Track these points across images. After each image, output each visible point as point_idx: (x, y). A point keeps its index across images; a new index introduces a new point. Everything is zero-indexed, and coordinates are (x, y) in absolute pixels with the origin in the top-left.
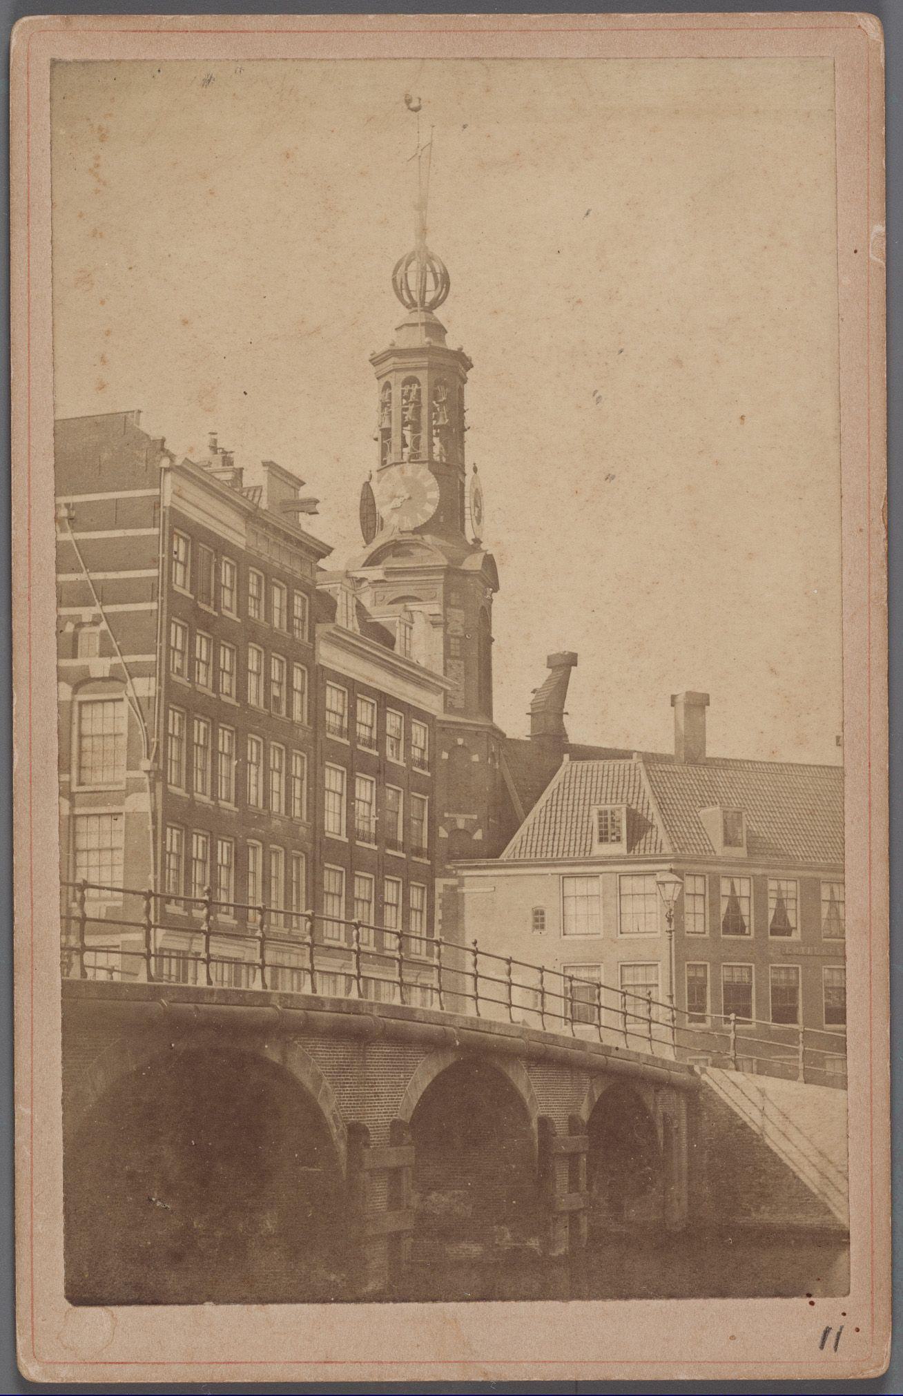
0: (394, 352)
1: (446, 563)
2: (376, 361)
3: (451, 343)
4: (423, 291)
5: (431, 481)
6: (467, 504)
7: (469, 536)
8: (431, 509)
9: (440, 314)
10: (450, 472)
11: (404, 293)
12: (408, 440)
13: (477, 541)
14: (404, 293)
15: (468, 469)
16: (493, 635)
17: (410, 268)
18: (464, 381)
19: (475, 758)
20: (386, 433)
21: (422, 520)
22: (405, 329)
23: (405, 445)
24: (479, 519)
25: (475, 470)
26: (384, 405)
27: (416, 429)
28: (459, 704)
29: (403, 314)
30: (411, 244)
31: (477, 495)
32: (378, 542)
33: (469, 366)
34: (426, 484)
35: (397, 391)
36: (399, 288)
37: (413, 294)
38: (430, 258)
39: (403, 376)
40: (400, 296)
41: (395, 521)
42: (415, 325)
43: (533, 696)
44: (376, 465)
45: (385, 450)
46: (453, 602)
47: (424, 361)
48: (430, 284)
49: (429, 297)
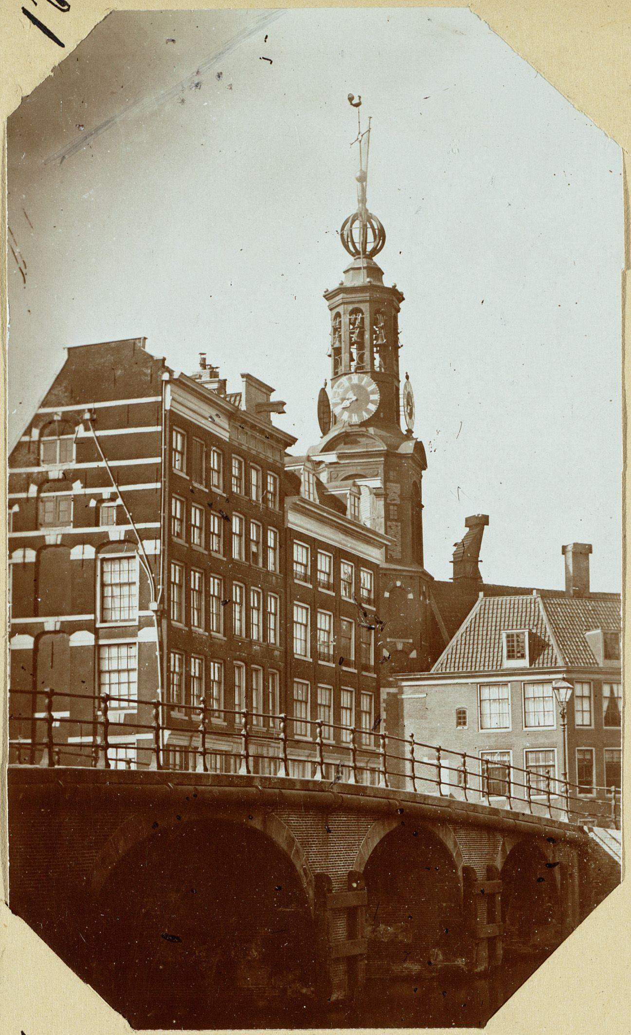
0: (342, 290)
1: (386, 448)
2: (328, 296)
3: (387, 282)
4: (365, 243)
5: (374, 386)
6: (402, 402)
7: (404, 428)
8: (373, 408)
9: (377, 259)
10: (388, 379)
11: (350, 244)
12: (355, 356)
13: (410, 431)
14: (350, 244)
15: (402, 377)
17: (354, 226)
18: (398, 310)
19: (411, 596)
20: (337, 351)
21: (366, 416)
22: (351, 272)
23: (352, 360)
24: (411, 415)
25: (407, 377)
26: (336, 330)
27: (361, 347)
28: (397, 555)
29: (349, 261)
30: (354, 208)
31: (409, 398)
32: (334, 432)
33: (400, 298)
34: (370, 389)
35: (345, 319)
36: (346, 241)
37: (357, 245)
39: (350, 307)
40: (347, 247)
41: (346, 418)
42: (359, 268)
43: (455, 548)
44: (330, 375)
45: (337, 364)
46: (392, 478)
47: (366, 296)
49: (369, 247)
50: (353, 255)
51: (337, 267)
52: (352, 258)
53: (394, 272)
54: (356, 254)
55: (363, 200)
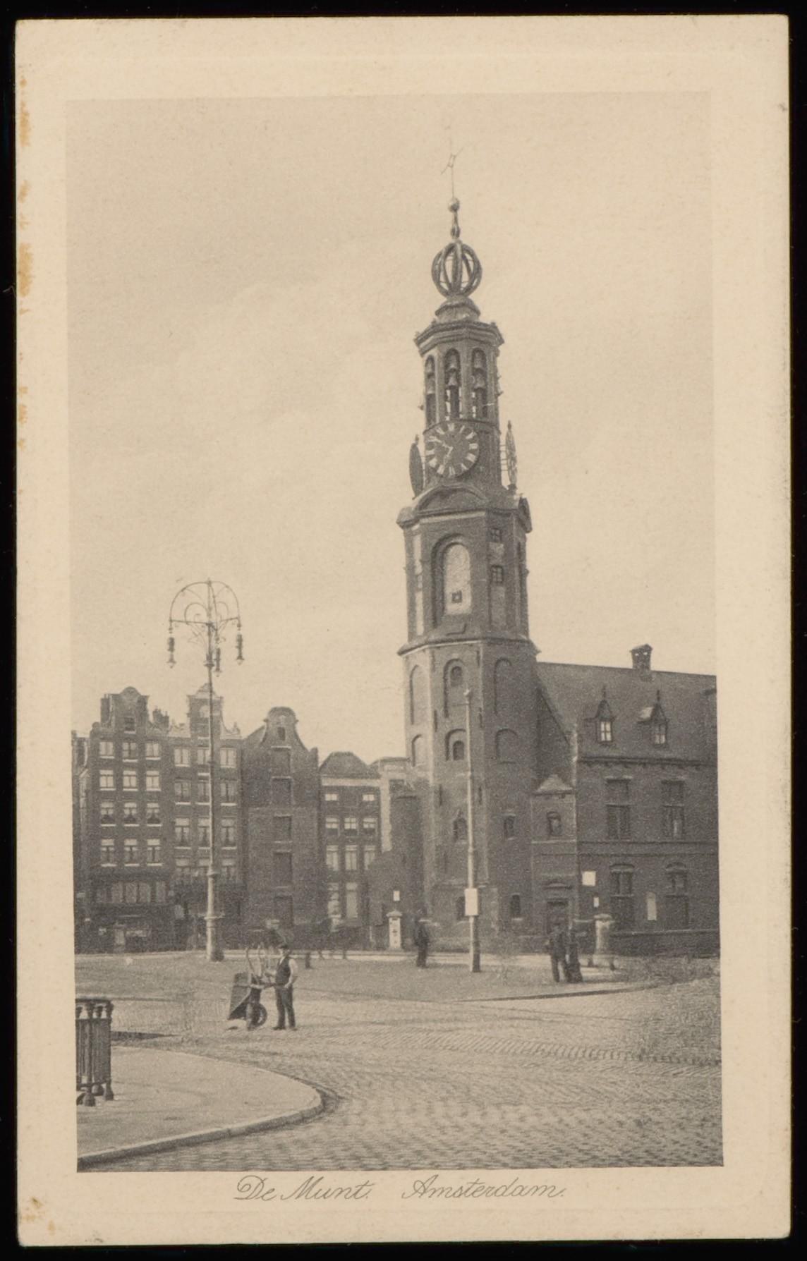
0: (434, 329)
7: (506, 482)
13: (513, 487)
15: (503, 427)
18: (497, 354)
20: (430, 398)
24: (513, 472)
25: (509, 426)
29: (442, 300)
31: (511, 448)
38: (466, 249)
40: (438, 282)
48: (465, 277)
55: (456, 233)
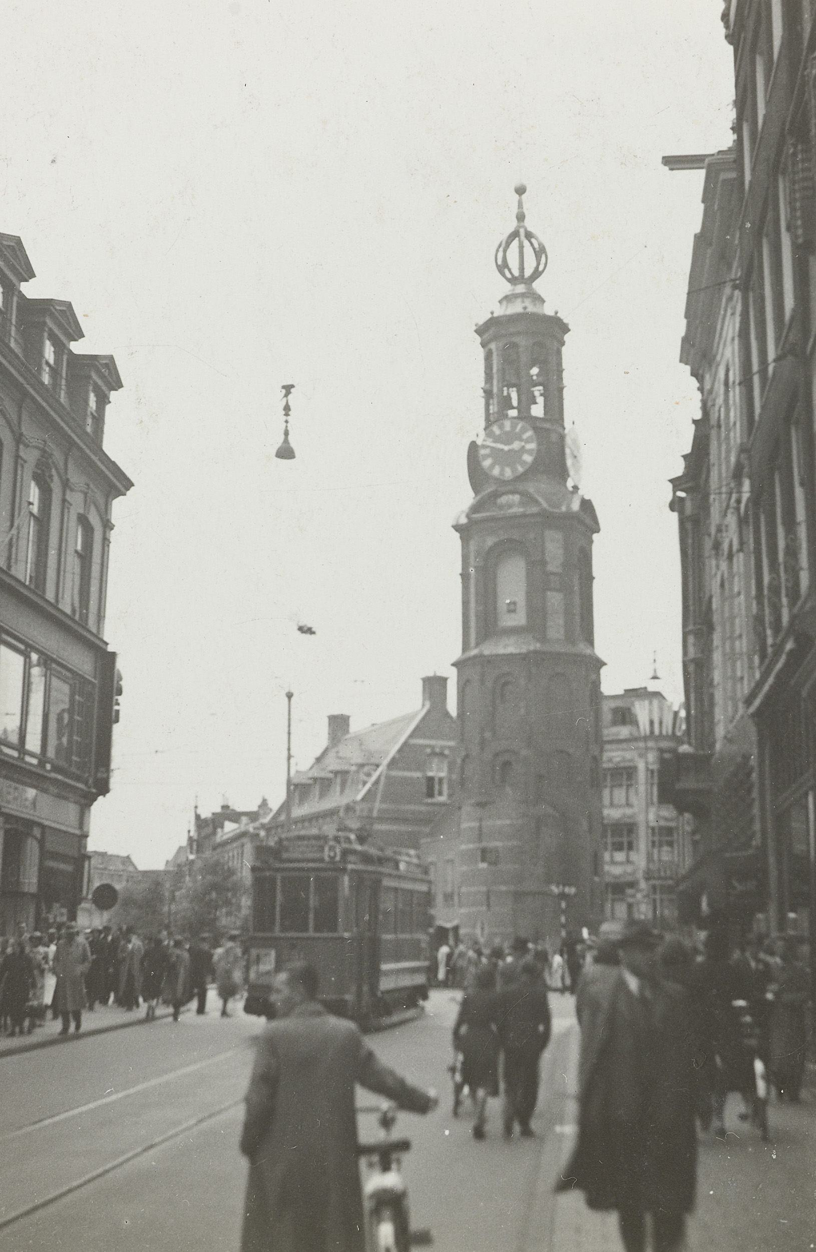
2: (480, 331)
9: (535, 285)
16: (595, 573)
18: (563, 344)
21: (520, 469)
29: (507, 288)
33: (565, 329)
36: (503, 267)
38: (529, 236)
49: (528, 272)
50: (509, 280)
51: (490, 297)
52: (509, 284)
53: (555, 296)
54: (513, 281)
55: (521, 217)
